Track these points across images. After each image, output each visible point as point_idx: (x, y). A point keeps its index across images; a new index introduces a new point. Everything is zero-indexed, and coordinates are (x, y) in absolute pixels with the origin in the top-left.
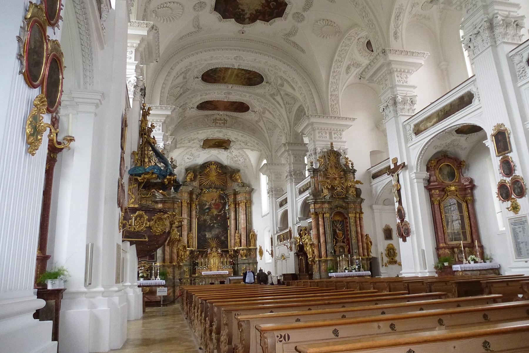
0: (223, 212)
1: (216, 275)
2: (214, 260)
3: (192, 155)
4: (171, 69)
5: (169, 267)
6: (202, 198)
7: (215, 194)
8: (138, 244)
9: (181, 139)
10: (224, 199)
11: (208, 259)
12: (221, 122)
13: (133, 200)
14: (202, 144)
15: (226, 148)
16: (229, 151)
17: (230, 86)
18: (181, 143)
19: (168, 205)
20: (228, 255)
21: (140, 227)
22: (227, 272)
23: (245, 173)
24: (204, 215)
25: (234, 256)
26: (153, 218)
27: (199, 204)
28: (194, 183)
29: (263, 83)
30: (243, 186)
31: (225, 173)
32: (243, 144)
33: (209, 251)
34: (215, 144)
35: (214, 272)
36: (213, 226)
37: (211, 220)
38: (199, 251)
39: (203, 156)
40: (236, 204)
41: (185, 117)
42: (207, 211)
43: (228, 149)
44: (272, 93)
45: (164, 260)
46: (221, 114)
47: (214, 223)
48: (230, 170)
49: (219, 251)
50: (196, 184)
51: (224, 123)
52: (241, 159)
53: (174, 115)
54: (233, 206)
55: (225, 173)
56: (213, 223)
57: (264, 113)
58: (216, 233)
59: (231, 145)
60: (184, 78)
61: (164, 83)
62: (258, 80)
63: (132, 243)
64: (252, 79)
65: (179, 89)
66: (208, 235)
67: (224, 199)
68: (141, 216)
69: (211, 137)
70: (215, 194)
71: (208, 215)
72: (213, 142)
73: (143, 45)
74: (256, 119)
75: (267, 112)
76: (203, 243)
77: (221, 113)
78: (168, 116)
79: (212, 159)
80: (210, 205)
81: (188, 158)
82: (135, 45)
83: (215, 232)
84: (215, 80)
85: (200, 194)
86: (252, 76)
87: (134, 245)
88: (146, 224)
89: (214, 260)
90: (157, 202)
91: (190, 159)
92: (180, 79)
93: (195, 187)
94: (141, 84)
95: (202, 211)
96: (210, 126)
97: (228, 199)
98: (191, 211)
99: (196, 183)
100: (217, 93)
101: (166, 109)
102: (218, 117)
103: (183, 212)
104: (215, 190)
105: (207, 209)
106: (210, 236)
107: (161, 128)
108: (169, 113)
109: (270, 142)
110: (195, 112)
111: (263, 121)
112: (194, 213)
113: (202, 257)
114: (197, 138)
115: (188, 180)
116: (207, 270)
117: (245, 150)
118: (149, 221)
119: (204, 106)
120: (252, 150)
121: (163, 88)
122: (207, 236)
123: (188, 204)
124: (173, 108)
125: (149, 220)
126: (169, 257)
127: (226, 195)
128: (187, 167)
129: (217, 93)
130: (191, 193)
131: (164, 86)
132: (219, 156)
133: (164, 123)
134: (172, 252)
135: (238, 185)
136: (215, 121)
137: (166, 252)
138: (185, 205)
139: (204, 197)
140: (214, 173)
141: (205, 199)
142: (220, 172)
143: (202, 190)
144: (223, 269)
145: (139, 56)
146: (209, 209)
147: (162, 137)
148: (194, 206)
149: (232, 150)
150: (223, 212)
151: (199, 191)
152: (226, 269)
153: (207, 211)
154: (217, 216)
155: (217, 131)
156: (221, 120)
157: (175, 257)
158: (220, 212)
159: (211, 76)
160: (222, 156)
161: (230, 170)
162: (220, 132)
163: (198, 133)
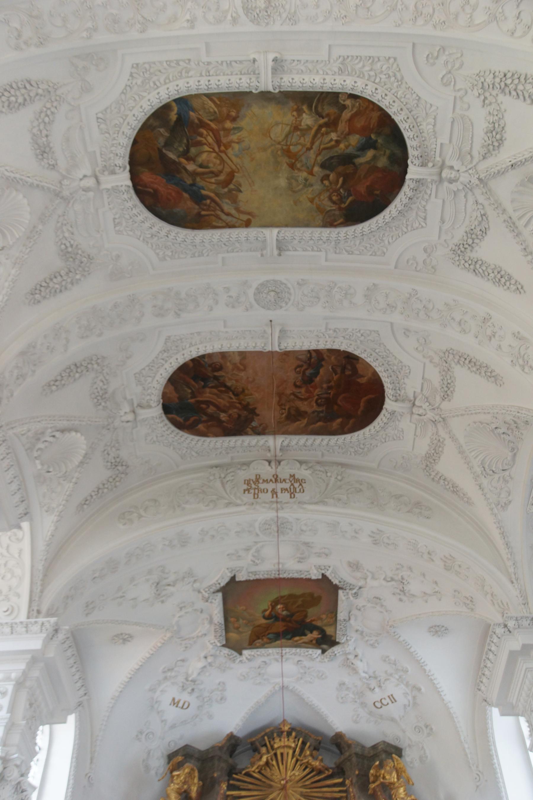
3: (191, 685)
15: (326, 642)
17: (271, 234)
23: (422, 759)
29: (413, 172)
34: (273, 617)
48: (358, 750)
51: (292, 495)
52: (399, 692)
55: (340, 771)
57: (447, 391)
59: (341, 615)
62: (382, 162)
72: (264, 605)
74: (423, 446)
75: (460, 373)
77: (274, 442)
81: (175, 703)
84: (198, 198)
86: (355, 140)
91: (185, 706)
109: (503, 535)
111: (453, 438)
114: (190, 573)
120: (438, 630)
128: (174, 748)
136: (253, 486)
140: (289, 772)
142: (316, 764)
149: (350, 641)
156: (276, 479)
163: (183, 541)
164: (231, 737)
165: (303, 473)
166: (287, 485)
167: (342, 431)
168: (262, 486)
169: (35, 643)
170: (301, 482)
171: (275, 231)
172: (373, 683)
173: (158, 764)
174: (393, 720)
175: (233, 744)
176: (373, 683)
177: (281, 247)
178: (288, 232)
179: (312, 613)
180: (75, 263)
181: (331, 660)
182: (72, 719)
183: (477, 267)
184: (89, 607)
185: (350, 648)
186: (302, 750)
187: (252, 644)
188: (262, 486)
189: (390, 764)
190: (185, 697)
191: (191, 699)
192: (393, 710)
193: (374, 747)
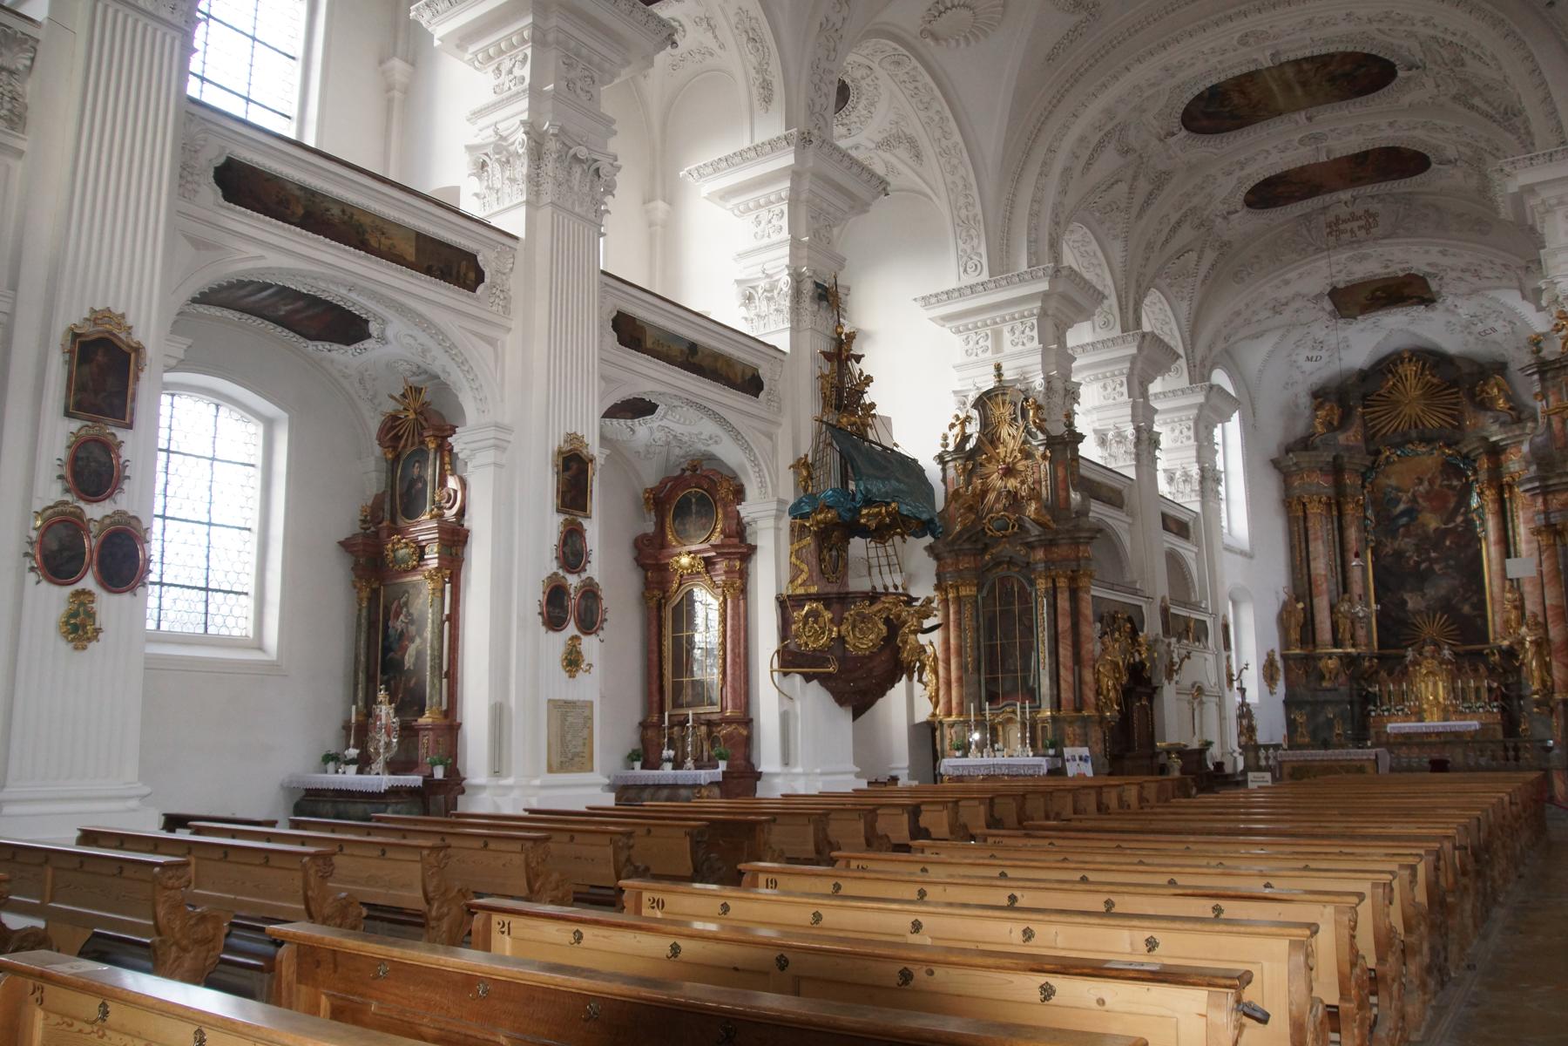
0: (1460, 519)
1: (1438, 734)
2: (1432, 689)
4: (1050, 150)
5: (1071, 723)
6: (1382, 481)
7: (1428, 459)
8: (825, 680)
9: (1238, 314)
10: (1460, 474)
11: (1411, 683)
12: (1355, 225)
13: (804, 576)
14: (1328, 305)
16: (1437, 305)
17: (1301, 117)
18: (1248, 322)
19: (1057, 552)
20: (1482, 668)
21: (817, 640)
22: (1473, 724)
24: (1394, 537)
25: (1505, 671)
26: (846, 615)
27: (1374, 502)
28: (1341, 438)
29: (1401, 74)
30: (1518, 420)
31: (1454, 383)
32: (1467, 276)
33: (1410, 654)
35: (1433, 723)
36: (1430, 570)
37: (1418, 549)
38: (1380, 658)
39: (1363, 342)
40: (1502, 489)
41: (1227, 244)
42: (1404, 520)
43: (1433, 301)
44: (1454, 91)
45: (1057, 704)
46: (1342, 200)
47: (1436, 561)
48: (1466, 369)
49: (1447, 653)
50: (1349, 437)
52: (1498, 325)
53: (1062, 287)
54: (1490, 494)
56: (1429, 559)
58: (1442, 592)
59: (1434, 286)
60: (1125, 152)
61: (1034, 201)
63: (808, 678)
64: (1360, 74)
65: (1123, 187)
66: (1413, 602)
67: (1460, 474)
68: (814, 614)
69: (1341, 281)
70: (1429, 461)
71: (1407, 534)
73: (806, 184)
76: (1395, 630)
77: (1345, 195)
78: (1045, 296)
79: (1399, 342)
80: (1414, 500)
82: (783, 194)
83: (1441, 587)
85: (1373, 467)
87: (815, 683)
88: (831, 631)
89: (1432, 689)
90: (1031, 546)
92: (1109, 160)
93: (1348, 448)
94: (808, 287)
95: (1386, 521)
96: (1318, 250)
97: (1475, 472)
98: (1341, 530)
99: (1350, 433)
100: (1276, 147)
101: (1034, 278)
102: (1343, 211)
103: (1311, 537)
104: (1421, 449)
105: (1403, 514)
106: (1422, 605)
107: (1035, 333)
108: (1043, 286)
110: (1249, 222)
112: (1352, 534)
113: (1389, 674)
115: (1320, 429)
116: (1407, 717)
117: (1492, 294)
118: (839, 625)
119: (1267, 194)
121: (1034, 215)
122: (1410, 605)
123: (1329, 505)
124: (1050, 272)
125: (838, 621)
126: (1071, 696)
127: (1466, 457)
128: (1315, 388)
129: (1276, 147)
130: (1336, 470)
131: (1036, 207)
132: (1412, 328)
133: (1043, 314)
134: (1079, 683)
135: (1496, 420)
136: (1334, 227)
137: (1063, 684)
138: (1314, 510)
139: (1388, 477)
141: (1393, 482)
142: (1435, 381)
143: (1378, 453)
144: (1462, 715)
145: (803, 211)
146: (1411, 512)
147: (1038, 358)
148: (1349, 508)
150: (1460, 519)
151: (1368, 461)
152: (1474, 712)
153: (1404, 520)
154: (1442, 534)
155: (1351, 259)
156: (1354, 217)
157: (1090, 695)
158: (1451, 518)
159: (1218, 110)
160: (1436, 328)
161: (1466, 369)
162: (1364, 258)
163: (1287, 283)
164: (1361, 371)
165: (1375, 207)
166: (1362, 223)
167: (1401, 177)
168: (1342, 227)
169: (1200, 399)
170: (1374, 216)
171: (1303, 113)
172: (1475, 320)
173: (1305, 400)
174: (1495, 342)
175: (1364, 376)
176: (1475, 320)
177: (1309, 119)
178: (1313, 111)
179: (1407, 291)
180: (1161, 180)
181: (1434, 309)
182: (1236, 417)
183: (1472, 107)
184: (1226, 339)
185: (1449, 301)
186: (1423, 369)
187: (1362, 313)
188: (1342, 227)
189: (1492, 381)
190: (1315, 354)
191: (1323, 353)
192: (1494, 336)
193: (1481, 365)
